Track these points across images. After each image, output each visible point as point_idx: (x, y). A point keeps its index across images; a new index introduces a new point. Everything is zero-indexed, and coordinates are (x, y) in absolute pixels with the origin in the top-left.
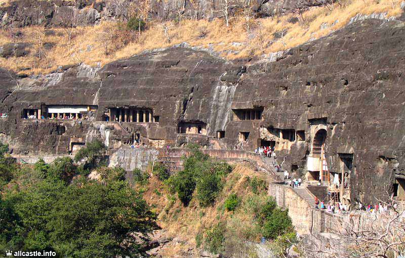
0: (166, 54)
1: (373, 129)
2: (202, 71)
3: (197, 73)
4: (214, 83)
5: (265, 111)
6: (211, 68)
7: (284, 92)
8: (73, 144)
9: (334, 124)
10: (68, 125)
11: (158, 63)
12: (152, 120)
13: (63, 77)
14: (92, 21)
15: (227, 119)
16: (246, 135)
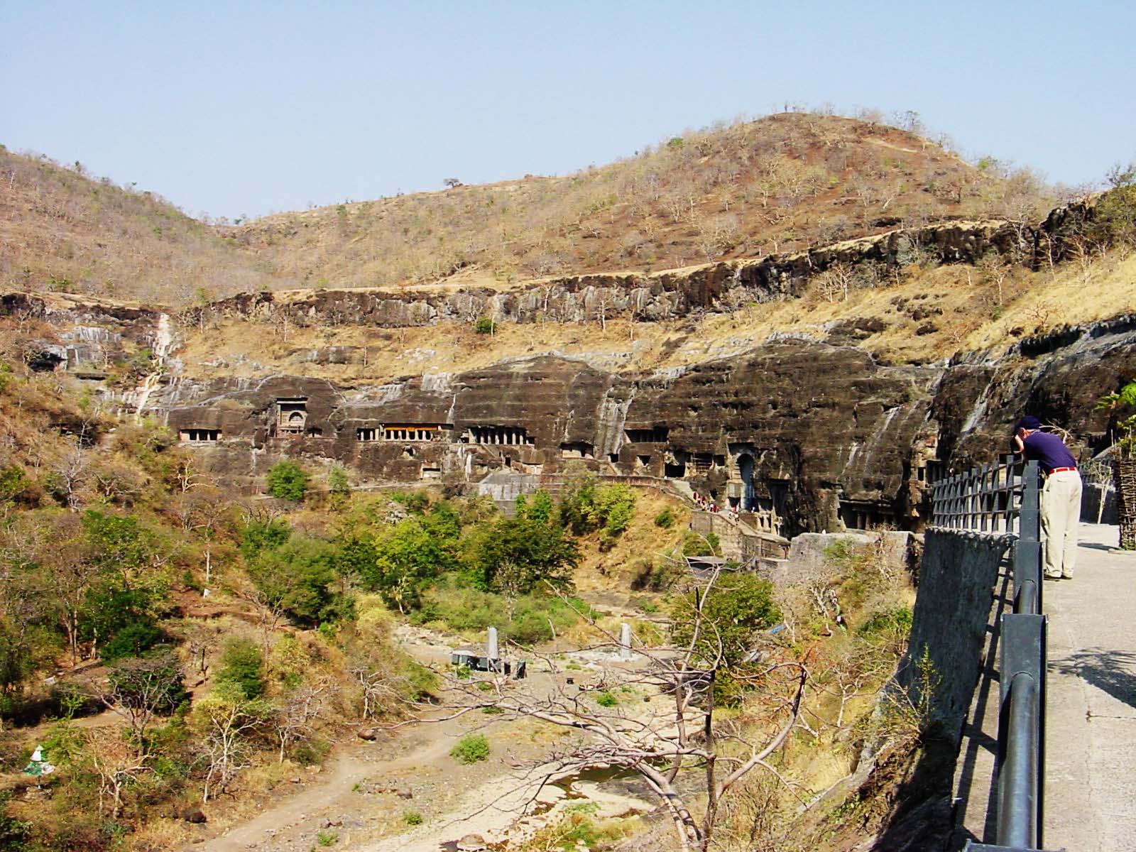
0: (532, 364)
1: (814, 456)
2: (583, 386)
3: (577, 387)
4: (599, 399)
5: (670, 433)
6: (594, 382)
7: (693, 414)
8: (425, 470)
9: (763, 450)
10: (417, 448)
11: (525, 377)
12: (525, 443)
13: (403, 390)
14: (427, 319)
15: (621, 441)
16: (645, 460)
